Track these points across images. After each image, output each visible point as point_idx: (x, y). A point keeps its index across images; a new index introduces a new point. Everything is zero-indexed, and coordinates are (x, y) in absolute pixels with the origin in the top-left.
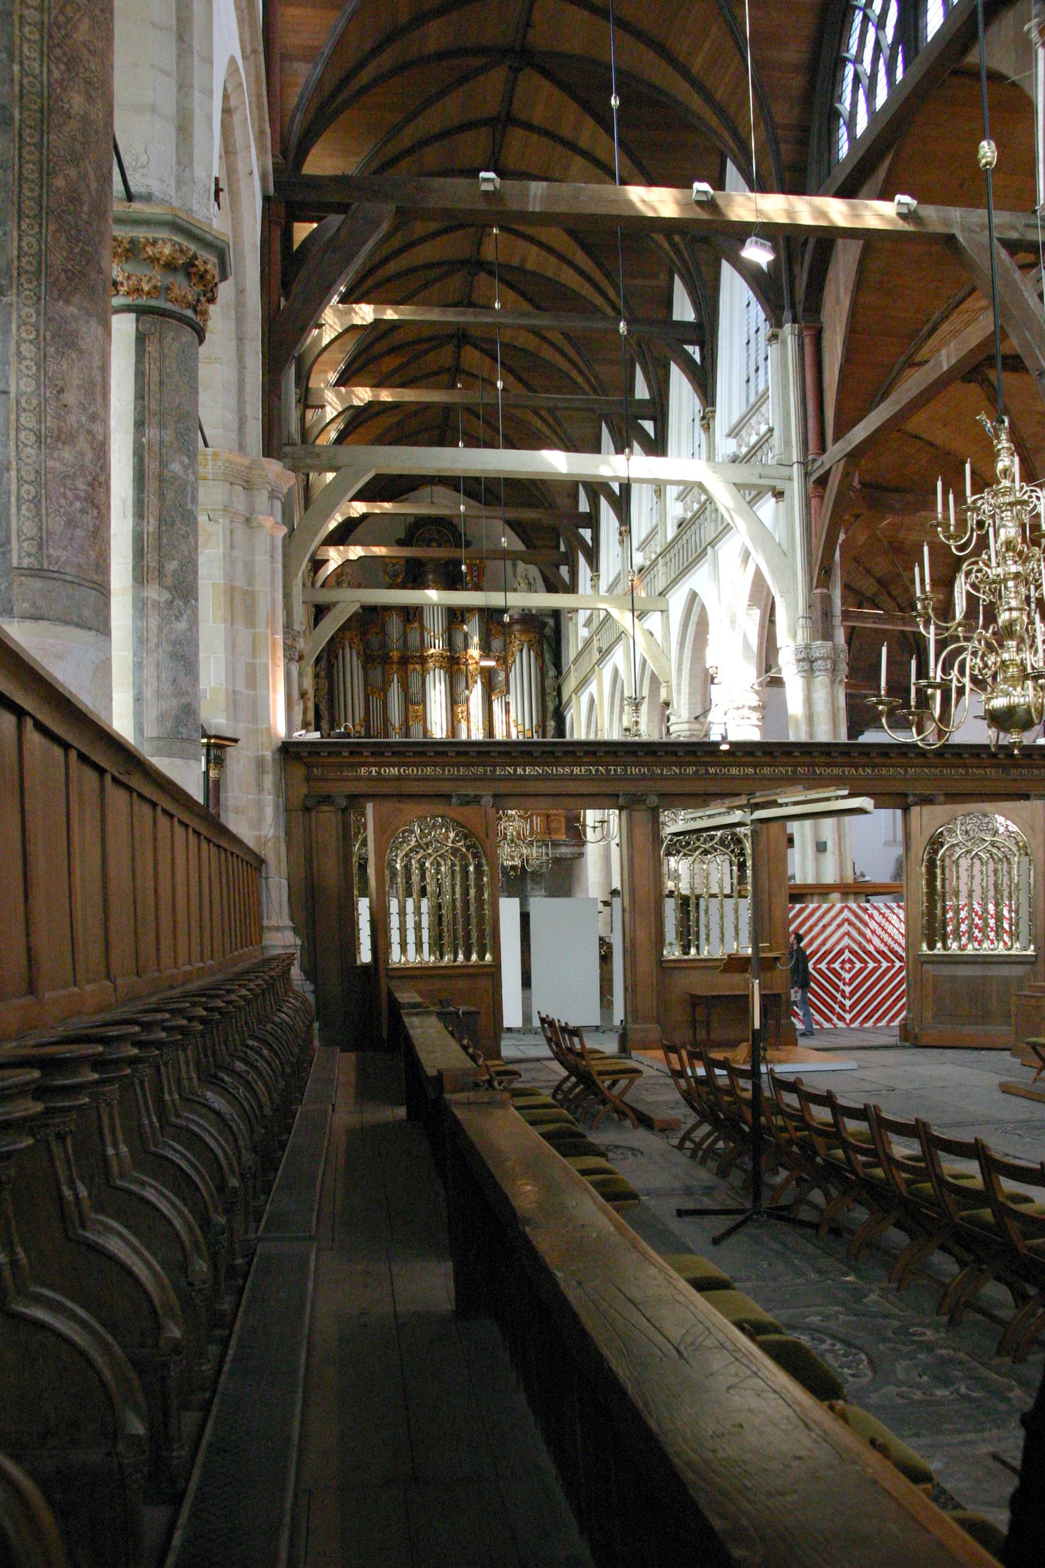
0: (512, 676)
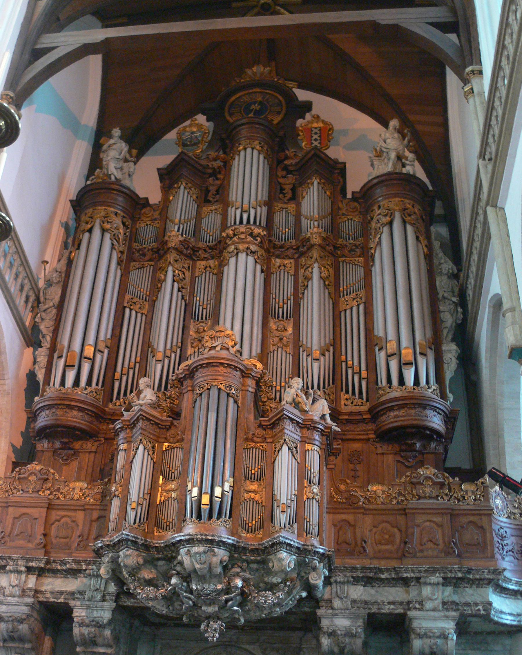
0: (376, 269)
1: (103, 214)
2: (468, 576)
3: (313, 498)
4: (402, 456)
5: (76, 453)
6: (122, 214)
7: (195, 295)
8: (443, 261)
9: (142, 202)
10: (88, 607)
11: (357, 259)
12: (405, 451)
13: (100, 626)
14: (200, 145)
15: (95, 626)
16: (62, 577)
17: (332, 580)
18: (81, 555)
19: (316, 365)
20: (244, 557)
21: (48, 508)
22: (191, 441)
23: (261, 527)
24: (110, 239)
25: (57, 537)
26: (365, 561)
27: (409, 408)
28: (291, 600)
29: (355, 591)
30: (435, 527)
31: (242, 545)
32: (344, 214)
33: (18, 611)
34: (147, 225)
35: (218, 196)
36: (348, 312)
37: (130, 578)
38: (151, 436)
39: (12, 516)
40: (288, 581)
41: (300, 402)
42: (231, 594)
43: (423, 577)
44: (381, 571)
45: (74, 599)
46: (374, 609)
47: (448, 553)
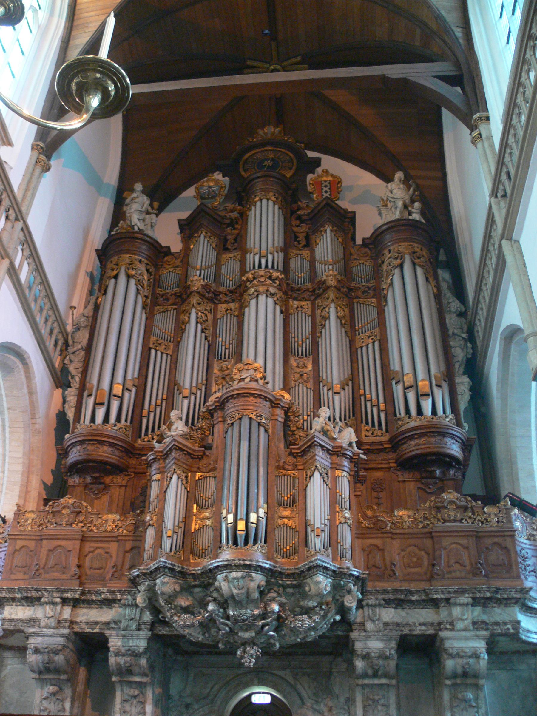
0: (389, 309)
1: (128, 261)
2: (496, 596)
3: (345, 522)
4: (423, 484)
5: (107, 488)
6: (146, 261)
7: (218, 336)
8: (450, 300)
9: (165, 250)
10: (124, 636)
11: (370, 300)
12: (426, 478)
13: (136, 655)
14: (217, 198)
15: (130, 655)
16: (97, 608)
17: (364, 603)
18: (116, 585)
19: (337, 398)
20: (280, 582)
21: (82, 540)
22: (224, 470)
23: (296, 551)
24: (136, 284)
25: (91, 568)
26: (395, 583)
27: (429, 437)
28: (325, 624)
29: (387, 613)
30: (462, 549)
31: (279, 569)
32: (355, 259)
33: (54, 642)
34: (170, 272)
35: (236, 244)
36: (364, 349)
37: (166, 606)
38: (184, 466)
39: (47, 549)
40: (323, 604)
41: (328, 430)
42: (268, 619)
43: (453, 597)
44: (411, 593)
45: (109, 629)
46: (406, 631)
47: (476, 574)
